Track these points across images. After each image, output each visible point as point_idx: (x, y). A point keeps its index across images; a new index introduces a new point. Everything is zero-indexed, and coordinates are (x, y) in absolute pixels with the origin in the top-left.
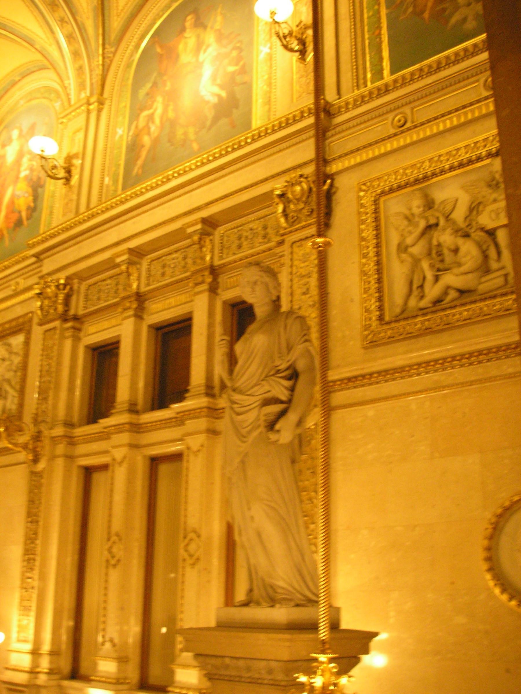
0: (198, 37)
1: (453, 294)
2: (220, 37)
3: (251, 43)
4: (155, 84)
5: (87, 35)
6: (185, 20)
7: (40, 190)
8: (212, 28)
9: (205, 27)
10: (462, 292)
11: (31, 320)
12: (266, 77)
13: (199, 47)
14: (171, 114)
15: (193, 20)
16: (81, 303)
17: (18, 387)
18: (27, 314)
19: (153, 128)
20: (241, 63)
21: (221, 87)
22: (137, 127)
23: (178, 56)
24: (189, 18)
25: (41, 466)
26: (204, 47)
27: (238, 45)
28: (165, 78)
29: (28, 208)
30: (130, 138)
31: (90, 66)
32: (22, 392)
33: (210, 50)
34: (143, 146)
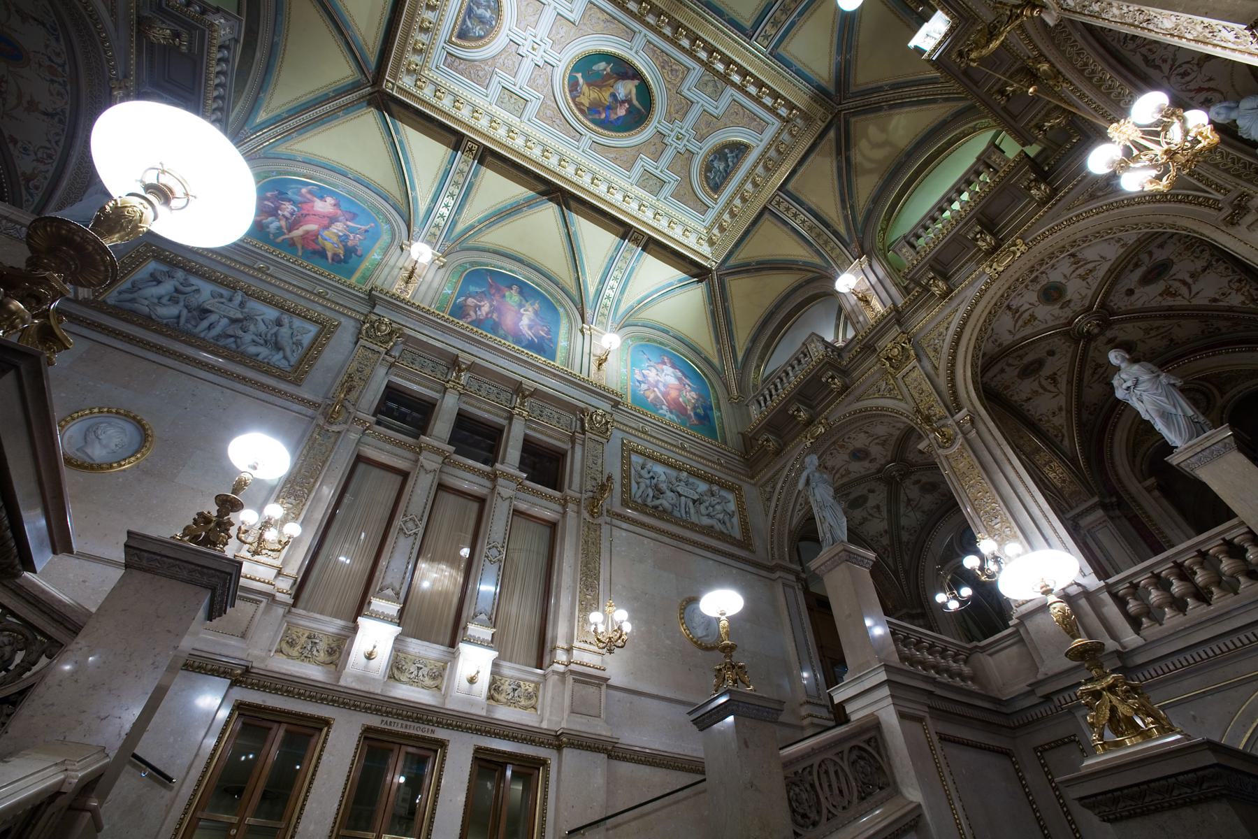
2: (536, 313)
3: (557, 333)
13: (521, 306)
14: (495, 316)
19: (479, 313)
22: (465, 300)
23: (504, 296)
29: (335, 255)
34: (468, 314)
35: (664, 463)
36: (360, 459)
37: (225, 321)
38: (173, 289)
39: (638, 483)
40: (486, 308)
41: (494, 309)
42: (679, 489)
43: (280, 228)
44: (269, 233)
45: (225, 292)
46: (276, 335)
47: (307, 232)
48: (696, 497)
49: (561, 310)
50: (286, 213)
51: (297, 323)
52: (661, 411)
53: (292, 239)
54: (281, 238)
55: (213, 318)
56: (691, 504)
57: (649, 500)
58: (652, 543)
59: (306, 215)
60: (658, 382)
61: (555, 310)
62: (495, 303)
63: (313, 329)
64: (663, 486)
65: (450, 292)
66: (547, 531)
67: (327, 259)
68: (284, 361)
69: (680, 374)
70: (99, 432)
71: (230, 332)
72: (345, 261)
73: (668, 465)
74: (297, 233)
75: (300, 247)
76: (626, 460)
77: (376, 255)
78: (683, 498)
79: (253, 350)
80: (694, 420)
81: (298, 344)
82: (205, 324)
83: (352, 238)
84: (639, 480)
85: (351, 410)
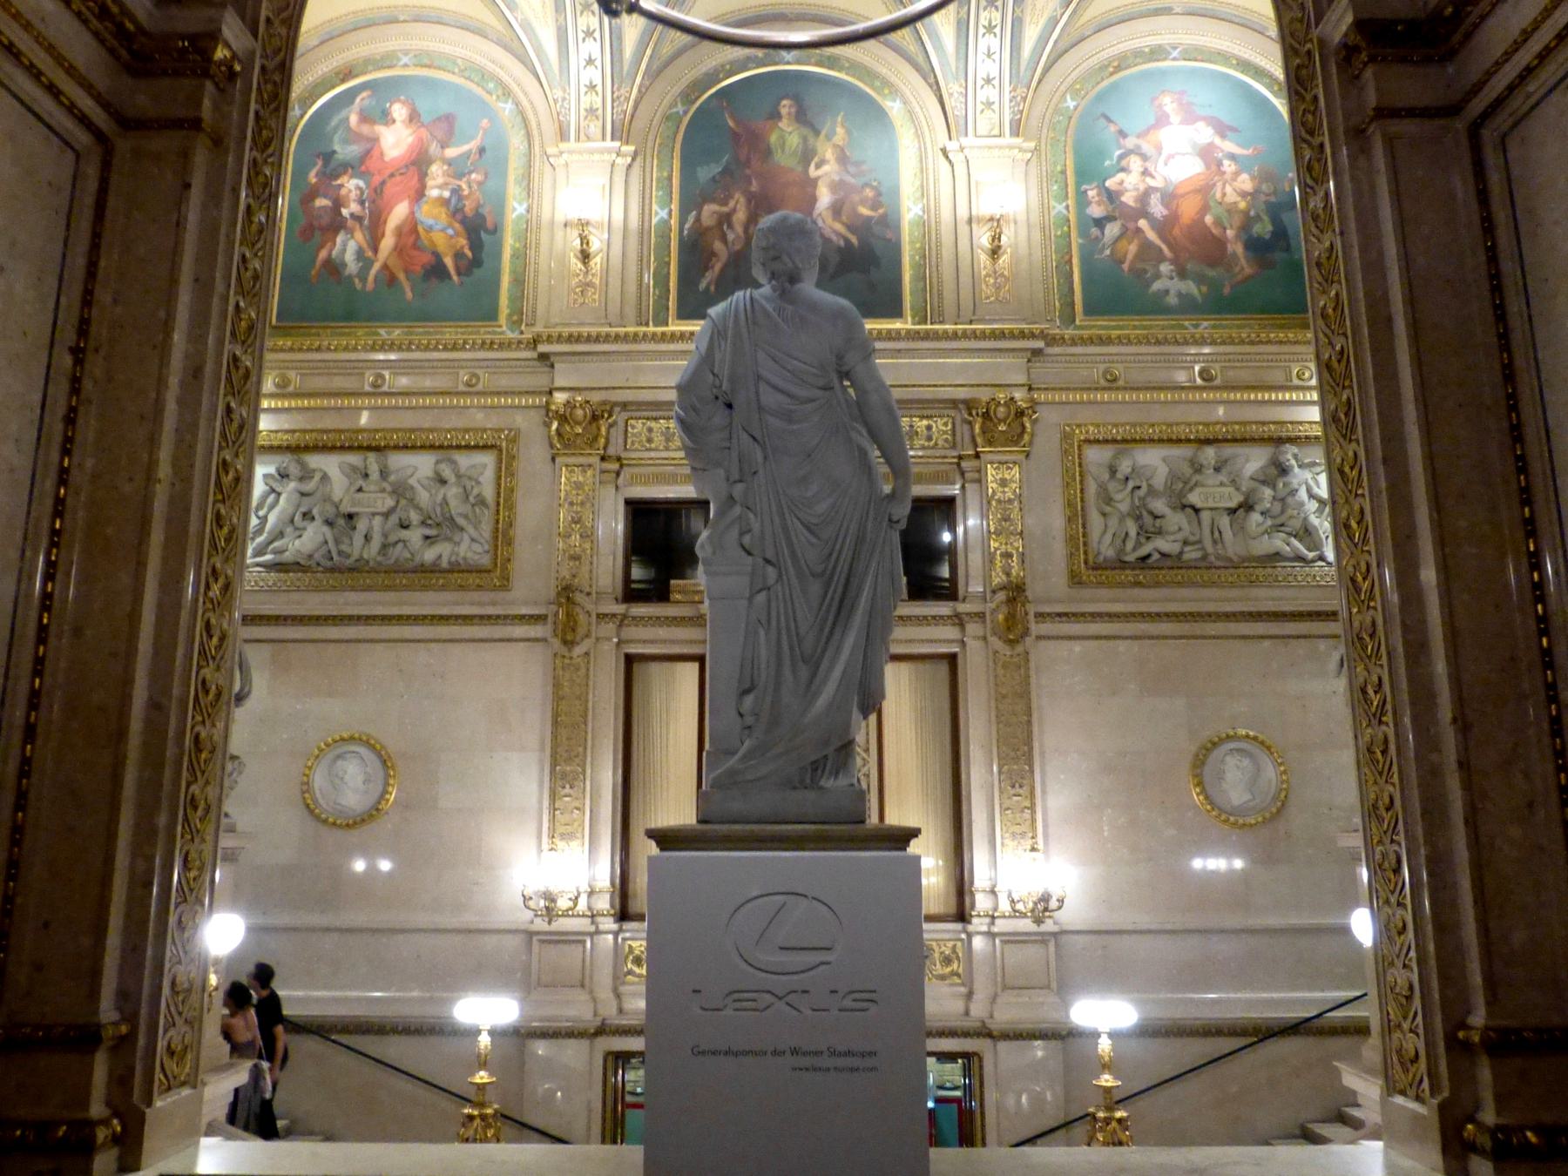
0: (805, 139)
1: (1156, 556)
4: (726, 171)
5: (621, 44)
6: (779, 104)
7: (483, 235)
8: (829, 138)
9: (817, 133)
10: (1164, 555)
11: (513, 440)
12: (918, 245)
15: (793, 110)
16: (621, 441)
17: (486, 529)
18: (510, 430)
19: (731, 236)
20: (881, 211)
21: (849, 227)
22: (698, 220)
24: (785, 102)
25: (578, 651)
26: (816, 159)
27: (875, 184)
28: (748, 172)
29: (458, 256)
30: (686, 232)
31: (613, 93)
32: (502, 537)
33: (826, 168)
34: (713, 254)
35: (1161, 441)
36: (630, 660)
37: (377, 521)
38: (298, 495)
39: (1104, 515)
40: (740, 216)
41: (760, 204)
42: (1194, 498)
43: (360, 254)
44: (350, 277)
45: (354, 459)
46: (445, 502)
47: (399, 232)
48: (1237, 499)
49: (893, 107)
50: (354, 207)
51: (464, 460)
52: (1157, 286)
53: (385, 267)
54: (371, 278)
55: (362, 526)
56: (1225, 522)
57: (1130, 545)
58: (1135, 646)
59: (383, 183)
60: (1144, 197)
61: (880, 115)
62: (755, 187)
63: (487, 459)
64: (1159, 506)
65: (664, 214)
66: (943, 669)
67: (450, 277)
68: (477, 547)
69: (1205, 134)
70: (340, 773)
71: (392, 538)
72: (476, 262)
73: (1170, 441)
74: (387, 243)
75: (401, 276)
76: (1075, 474)
77: (516, 209)
78: (1205, 516)
79: (429, 555)
80: (1244, 265)
81: (481, 502)
82: (358, 539)
83: (464, 186)
84: (1108, 509)
85: (590, 607)
